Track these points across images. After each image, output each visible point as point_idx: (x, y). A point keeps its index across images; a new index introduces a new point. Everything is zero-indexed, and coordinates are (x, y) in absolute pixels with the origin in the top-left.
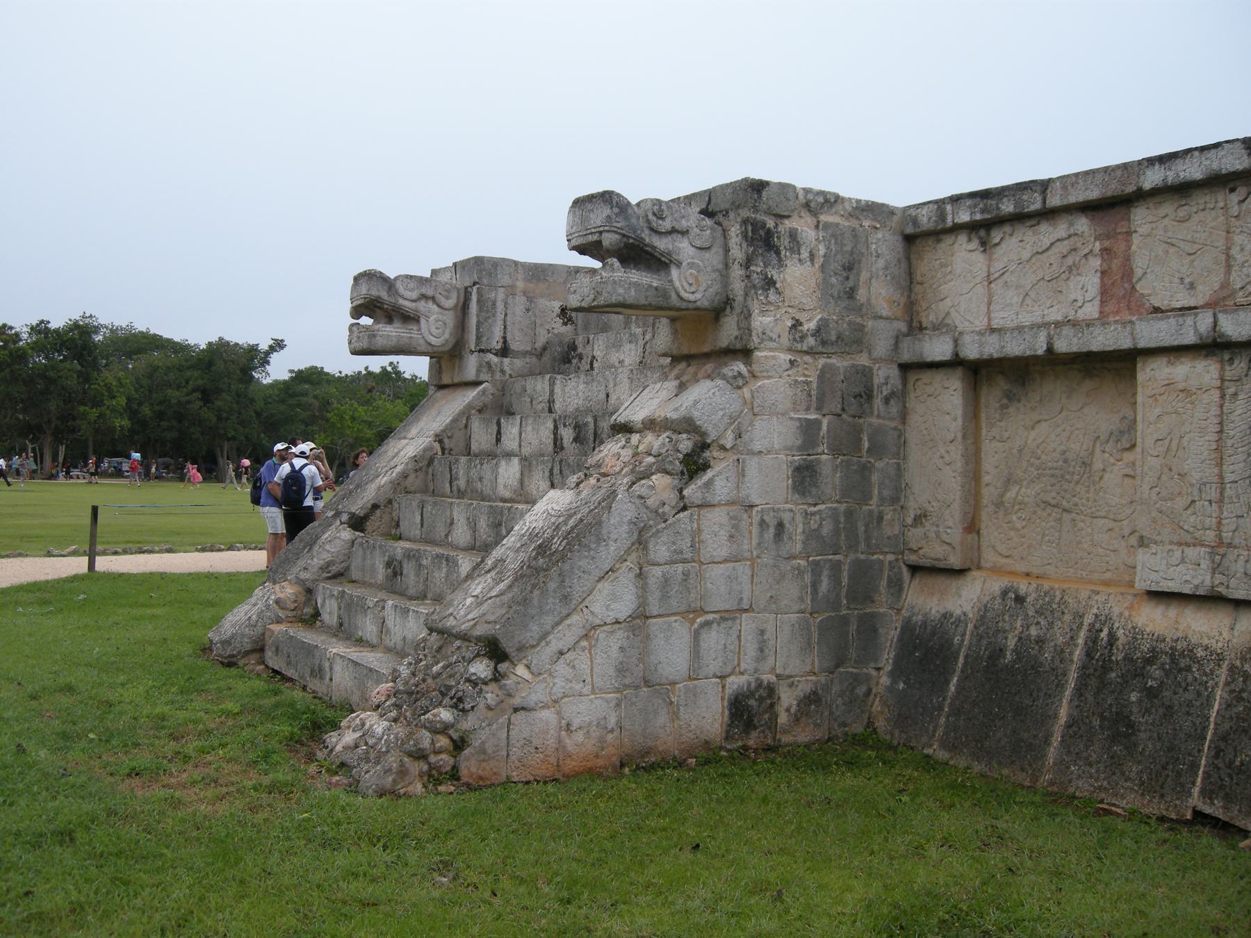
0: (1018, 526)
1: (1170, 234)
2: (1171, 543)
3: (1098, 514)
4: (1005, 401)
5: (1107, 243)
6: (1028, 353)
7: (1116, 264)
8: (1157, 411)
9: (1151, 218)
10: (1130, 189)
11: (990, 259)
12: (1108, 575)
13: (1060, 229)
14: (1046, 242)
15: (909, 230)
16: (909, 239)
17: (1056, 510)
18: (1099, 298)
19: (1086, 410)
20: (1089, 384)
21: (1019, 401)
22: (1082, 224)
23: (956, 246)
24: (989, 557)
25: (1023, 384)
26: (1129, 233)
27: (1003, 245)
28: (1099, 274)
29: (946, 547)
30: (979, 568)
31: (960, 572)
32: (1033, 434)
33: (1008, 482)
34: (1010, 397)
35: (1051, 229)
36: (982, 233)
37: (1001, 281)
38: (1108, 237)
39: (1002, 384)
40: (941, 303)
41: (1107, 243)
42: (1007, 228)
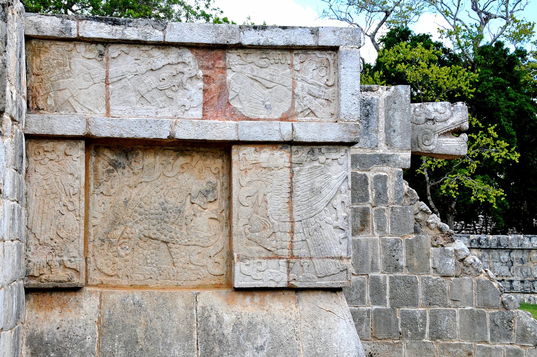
0: (122, 253)
1: (255, 74)
2: (260, 258)
3: (188, 243)
4: (111, 168)
5: (208, 73)
6: (154, 137)
7: (213, 86)
8: (248, 179)
9: (241, 62)
10: (233, 42)
11: (107, 66)
12: (198, 282)
13: (173, 55)
14: (159, 64)
15: (32, 32)
16: (28, 38)
17: (156, 241)
18: (202, 106)
19: (180, 177)
20: (182, 160)
21: (124, 168)
22: (188, 56)
23: (74, 53)
24: (96, 277)
25: (127, 157)
26: (224, 68)
27: (120, 60)
28: (201, 91)
29: (69, 272)
30: (87, 284)
31: (76, 289)
32: (136, 191)
33: (115, 223)
34: (115, 166)
35: (163, 56)
36: (100, 47)
37: (119, 85)
38: (208, 68)
39: (109, 155)
40: (59, 93)
41: (208, 73)
42: (125, 48)
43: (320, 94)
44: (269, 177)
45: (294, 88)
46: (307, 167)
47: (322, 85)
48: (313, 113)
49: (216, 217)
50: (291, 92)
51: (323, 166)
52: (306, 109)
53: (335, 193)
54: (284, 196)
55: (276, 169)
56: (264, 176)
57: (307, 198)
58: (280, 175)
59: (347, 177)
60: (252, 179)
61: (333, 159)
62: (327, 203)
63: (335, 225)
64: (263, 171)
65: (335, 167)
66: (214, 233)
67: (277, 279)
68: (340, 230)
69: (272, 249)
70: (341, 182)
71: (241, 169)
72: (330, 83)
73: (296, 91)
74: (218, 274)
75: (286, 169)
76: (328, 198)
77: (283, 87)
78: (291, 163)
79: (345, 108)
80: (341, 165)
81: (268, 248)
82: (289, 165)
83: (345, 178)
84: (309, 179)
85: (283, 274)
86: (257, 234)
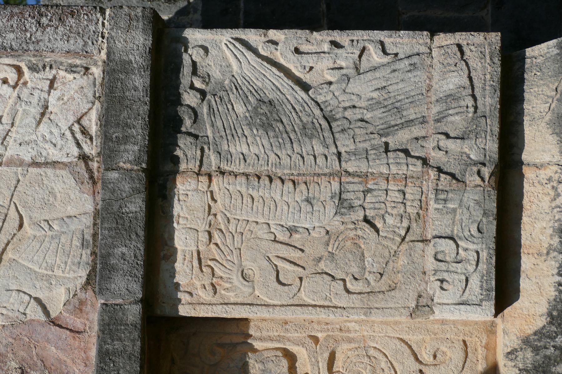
8: (237, 280)
43: (35, 100)
44: (232, 228)
45: (21, 163)
46: (209, 133)
47: (15, 94)
48: (81, 117)
49: (326, 355)
50: (30, 169)
51: (208, 97)
52: (73, 133)
53: (274, 70)
54: (279, 192)
55: (213, 211)
56: (229, 241)
57: (285, 136)
58: (227, 201)
59: (237, 39)
60: (235, 269)
61: (195, 72)
62: (297, 88)
63: (351, 72)
64: (219, 242)
65: (211, 66)
66: (366, 360)
67: (478, 214)
68: (364, 58)
69: (405, 224)
70: (250, 55)
71: (211, 292)
72: (12, 76)
73: (27, 159)
74: (462, 355)
75: (215, 187)
76: (285, 84)
77: (19, 188)
78: (198, 174)
79: (72, 42)
80: (206, 50)
81: (403, 233)
82: (204, 179)
83: (237, 44)
84: (240, 131)
85: (465, 199)
86: (368, 259)
